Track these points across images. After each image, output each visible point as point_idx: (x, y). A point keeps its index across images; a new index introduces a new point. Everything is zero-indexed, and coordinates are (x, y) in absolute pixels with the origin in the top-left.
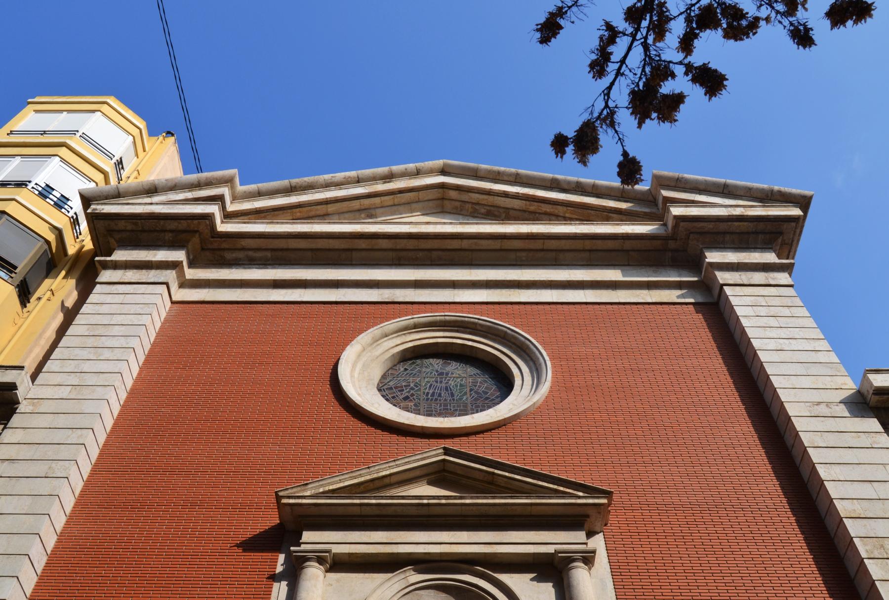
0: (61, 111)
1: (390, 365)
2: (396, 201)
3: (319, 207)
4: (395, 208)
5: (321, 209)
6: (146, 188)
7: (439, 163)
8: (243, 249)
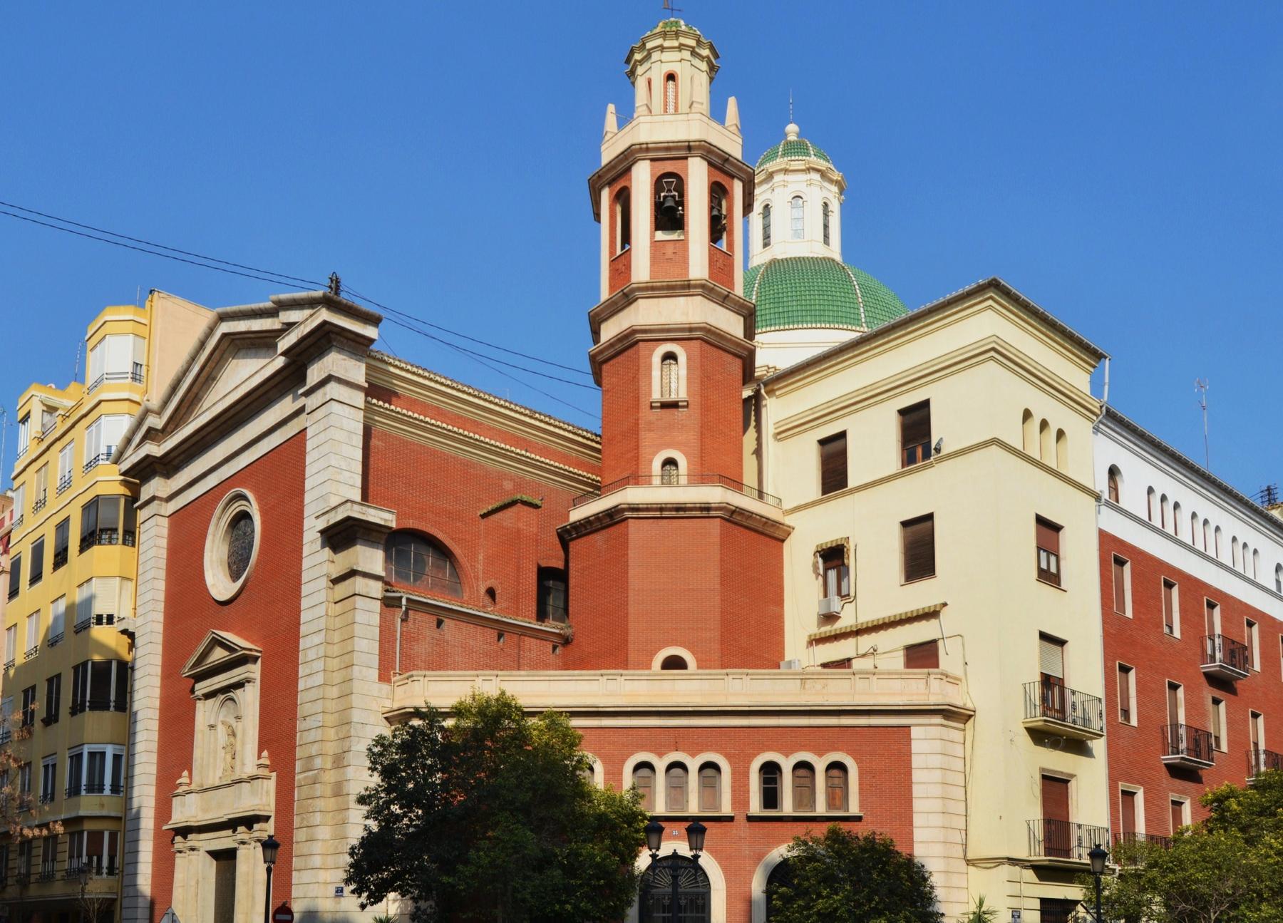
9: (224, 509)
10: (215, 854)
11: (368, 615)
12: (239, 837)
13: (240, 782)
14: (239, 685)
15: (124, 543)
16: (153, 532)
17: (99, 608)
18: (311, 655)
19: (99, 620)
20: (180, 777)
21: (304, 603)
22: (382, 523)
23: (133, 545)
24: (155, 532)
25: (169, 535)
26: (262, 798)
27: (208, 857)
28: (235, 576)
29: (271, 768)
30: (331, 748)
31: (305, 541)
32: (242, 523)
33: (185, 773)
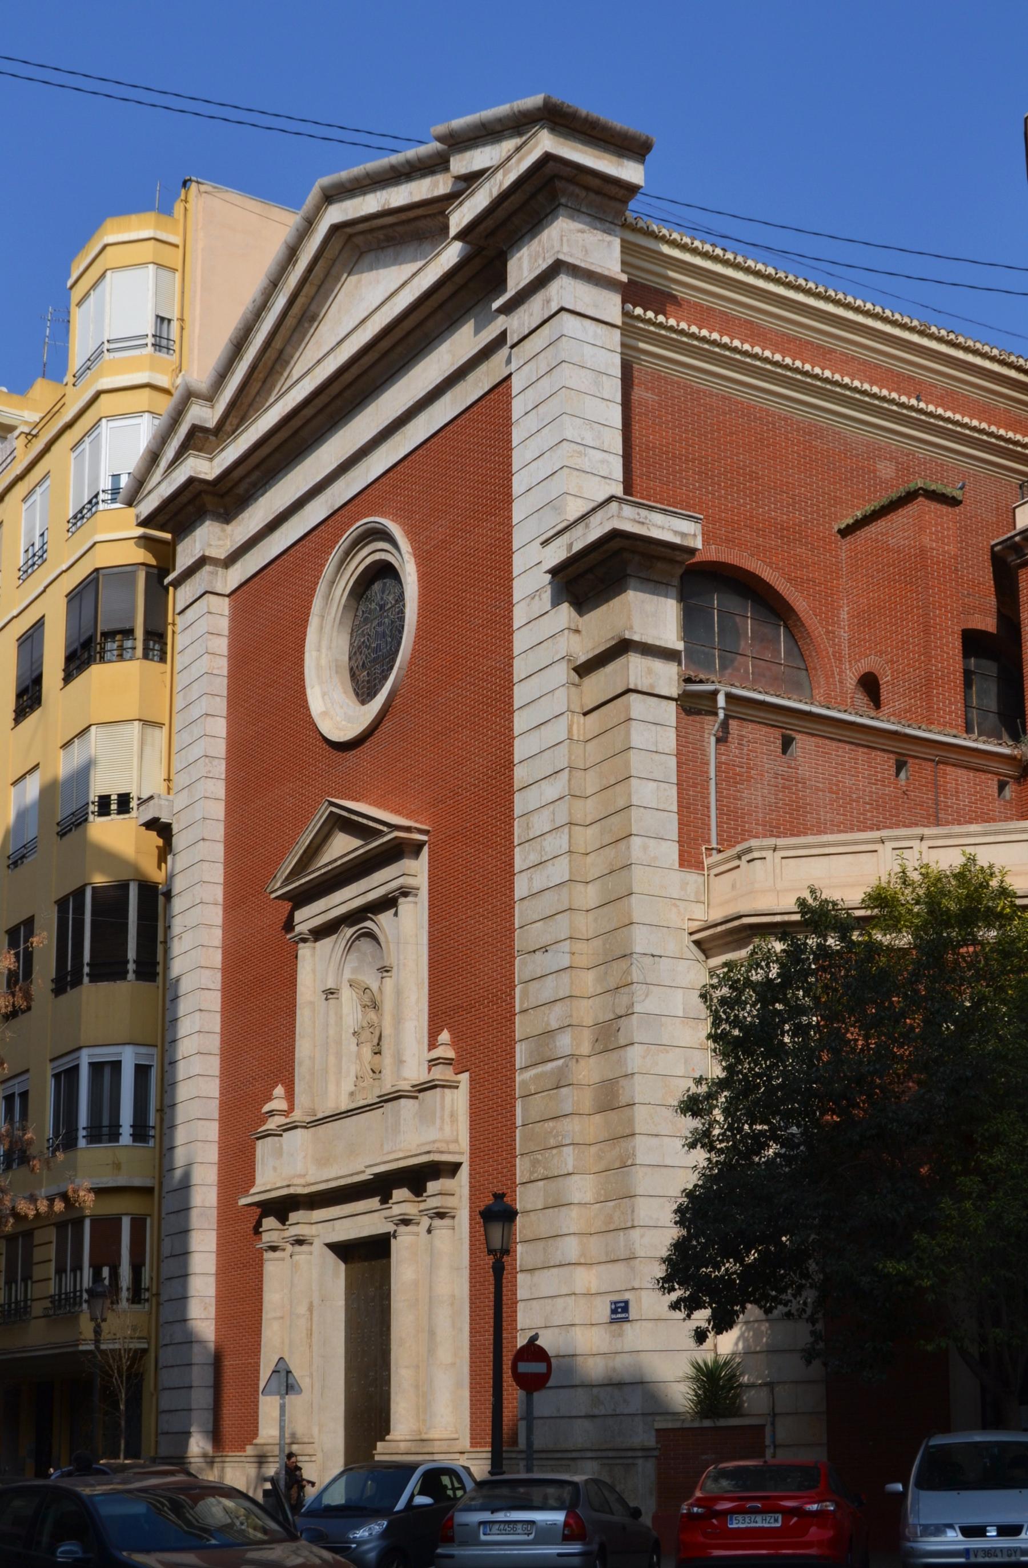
0: (87, 295)
1: (351, 615)
2: (317, 282)
3: (267, 355)
4: (322, 290)
5: (271, 354)
6: (149, 459)
7: (313, 196)
8: (242, 479)
9: (342, 562)
10: (343, 1250)
11: (655, 731)
12: (397, 1210)
13: (395, 1097)
14: (388, 903)
15: (146, 656)
16: (202, 627)
17: (102, 784)
18: (541, 823)
19: (104, 805)
20: (269, 1098)
21: (521, 722)
22: (677, 540)
23: (163, 659)
24: (204, 628)
25: (231, 630)
26: (444, 1127)
27: (330, 1256)
28: (364, 693)
29: (458, 1065)
30: (588, 1012)
31: (517, 596)
32: (377, 586)
33: (279, 1091)
